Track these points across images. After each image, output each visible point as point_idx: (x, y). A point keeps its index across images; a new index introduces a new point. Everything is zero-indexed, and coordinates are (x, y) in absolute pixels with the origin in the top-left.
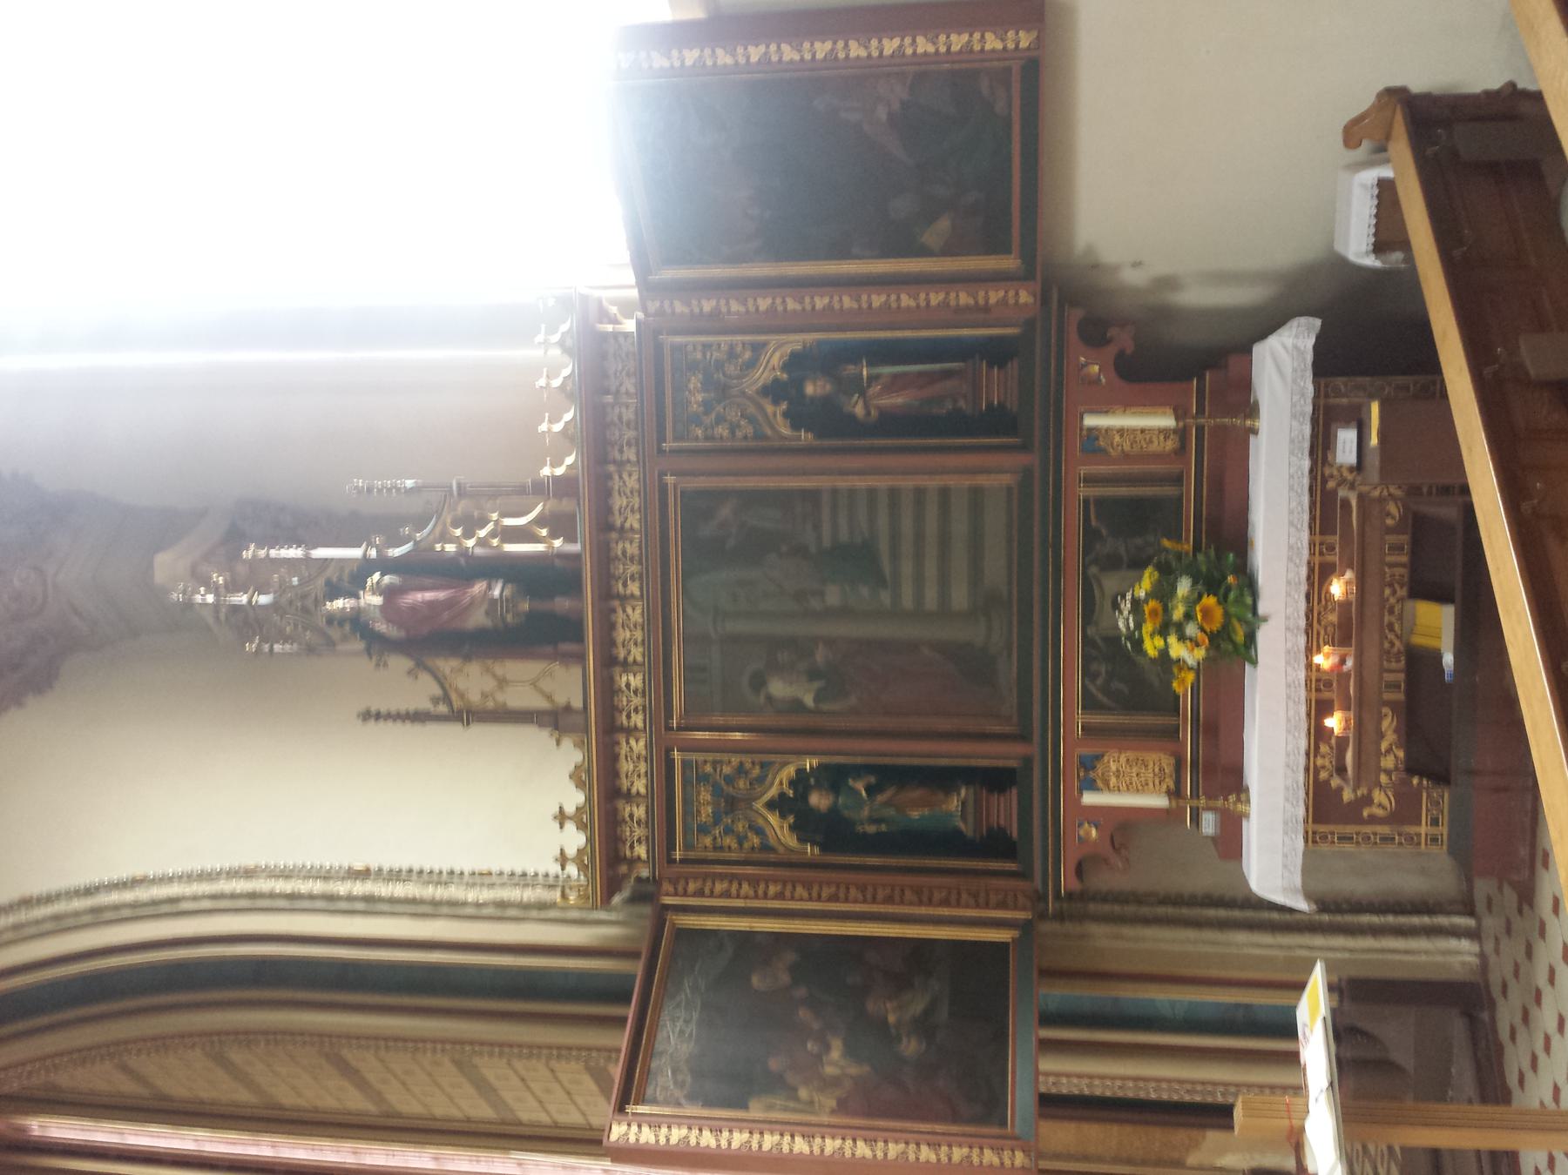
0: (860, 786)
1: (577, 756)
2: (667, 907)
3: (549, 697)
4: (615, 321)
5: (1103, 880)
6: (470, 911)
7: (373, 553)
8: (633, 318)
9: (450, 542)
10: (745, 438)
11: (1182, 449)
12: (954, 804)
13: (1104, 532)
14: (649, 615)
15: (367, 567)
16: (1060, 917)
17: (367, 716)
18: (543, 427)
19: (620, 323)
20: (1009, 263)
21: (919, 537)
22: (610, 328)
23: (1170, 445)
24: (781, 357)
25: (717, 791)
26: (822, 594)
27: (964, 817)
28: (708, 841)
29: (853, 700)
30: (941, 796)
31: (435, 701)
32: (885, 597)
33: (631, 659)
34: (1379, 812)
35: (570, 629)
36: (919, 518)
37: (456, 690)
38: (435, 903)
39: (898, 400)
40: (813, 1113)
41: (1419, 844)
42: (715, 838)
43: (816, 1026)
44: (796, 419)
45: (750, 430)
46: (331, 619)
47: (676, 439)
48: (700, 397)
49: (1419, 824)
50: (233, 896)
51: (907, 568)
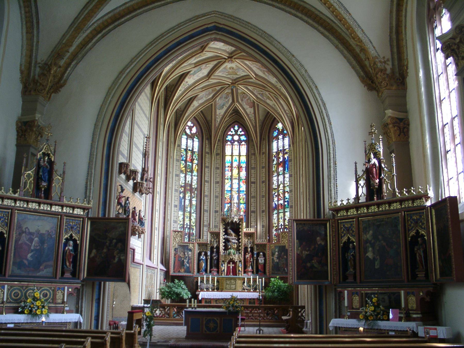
2: (330, 221)
6: (329, 185)
10: (408, 228)
12: (352, 270)
17: (356, 163)
18: (405, 189)
25: (350, 227)
28: (342, 226)
30: (352, 268)
38: (330, 179)
40: (297, 250)
43: (311, 249)
44: (413, 237)
47: (407, 214)
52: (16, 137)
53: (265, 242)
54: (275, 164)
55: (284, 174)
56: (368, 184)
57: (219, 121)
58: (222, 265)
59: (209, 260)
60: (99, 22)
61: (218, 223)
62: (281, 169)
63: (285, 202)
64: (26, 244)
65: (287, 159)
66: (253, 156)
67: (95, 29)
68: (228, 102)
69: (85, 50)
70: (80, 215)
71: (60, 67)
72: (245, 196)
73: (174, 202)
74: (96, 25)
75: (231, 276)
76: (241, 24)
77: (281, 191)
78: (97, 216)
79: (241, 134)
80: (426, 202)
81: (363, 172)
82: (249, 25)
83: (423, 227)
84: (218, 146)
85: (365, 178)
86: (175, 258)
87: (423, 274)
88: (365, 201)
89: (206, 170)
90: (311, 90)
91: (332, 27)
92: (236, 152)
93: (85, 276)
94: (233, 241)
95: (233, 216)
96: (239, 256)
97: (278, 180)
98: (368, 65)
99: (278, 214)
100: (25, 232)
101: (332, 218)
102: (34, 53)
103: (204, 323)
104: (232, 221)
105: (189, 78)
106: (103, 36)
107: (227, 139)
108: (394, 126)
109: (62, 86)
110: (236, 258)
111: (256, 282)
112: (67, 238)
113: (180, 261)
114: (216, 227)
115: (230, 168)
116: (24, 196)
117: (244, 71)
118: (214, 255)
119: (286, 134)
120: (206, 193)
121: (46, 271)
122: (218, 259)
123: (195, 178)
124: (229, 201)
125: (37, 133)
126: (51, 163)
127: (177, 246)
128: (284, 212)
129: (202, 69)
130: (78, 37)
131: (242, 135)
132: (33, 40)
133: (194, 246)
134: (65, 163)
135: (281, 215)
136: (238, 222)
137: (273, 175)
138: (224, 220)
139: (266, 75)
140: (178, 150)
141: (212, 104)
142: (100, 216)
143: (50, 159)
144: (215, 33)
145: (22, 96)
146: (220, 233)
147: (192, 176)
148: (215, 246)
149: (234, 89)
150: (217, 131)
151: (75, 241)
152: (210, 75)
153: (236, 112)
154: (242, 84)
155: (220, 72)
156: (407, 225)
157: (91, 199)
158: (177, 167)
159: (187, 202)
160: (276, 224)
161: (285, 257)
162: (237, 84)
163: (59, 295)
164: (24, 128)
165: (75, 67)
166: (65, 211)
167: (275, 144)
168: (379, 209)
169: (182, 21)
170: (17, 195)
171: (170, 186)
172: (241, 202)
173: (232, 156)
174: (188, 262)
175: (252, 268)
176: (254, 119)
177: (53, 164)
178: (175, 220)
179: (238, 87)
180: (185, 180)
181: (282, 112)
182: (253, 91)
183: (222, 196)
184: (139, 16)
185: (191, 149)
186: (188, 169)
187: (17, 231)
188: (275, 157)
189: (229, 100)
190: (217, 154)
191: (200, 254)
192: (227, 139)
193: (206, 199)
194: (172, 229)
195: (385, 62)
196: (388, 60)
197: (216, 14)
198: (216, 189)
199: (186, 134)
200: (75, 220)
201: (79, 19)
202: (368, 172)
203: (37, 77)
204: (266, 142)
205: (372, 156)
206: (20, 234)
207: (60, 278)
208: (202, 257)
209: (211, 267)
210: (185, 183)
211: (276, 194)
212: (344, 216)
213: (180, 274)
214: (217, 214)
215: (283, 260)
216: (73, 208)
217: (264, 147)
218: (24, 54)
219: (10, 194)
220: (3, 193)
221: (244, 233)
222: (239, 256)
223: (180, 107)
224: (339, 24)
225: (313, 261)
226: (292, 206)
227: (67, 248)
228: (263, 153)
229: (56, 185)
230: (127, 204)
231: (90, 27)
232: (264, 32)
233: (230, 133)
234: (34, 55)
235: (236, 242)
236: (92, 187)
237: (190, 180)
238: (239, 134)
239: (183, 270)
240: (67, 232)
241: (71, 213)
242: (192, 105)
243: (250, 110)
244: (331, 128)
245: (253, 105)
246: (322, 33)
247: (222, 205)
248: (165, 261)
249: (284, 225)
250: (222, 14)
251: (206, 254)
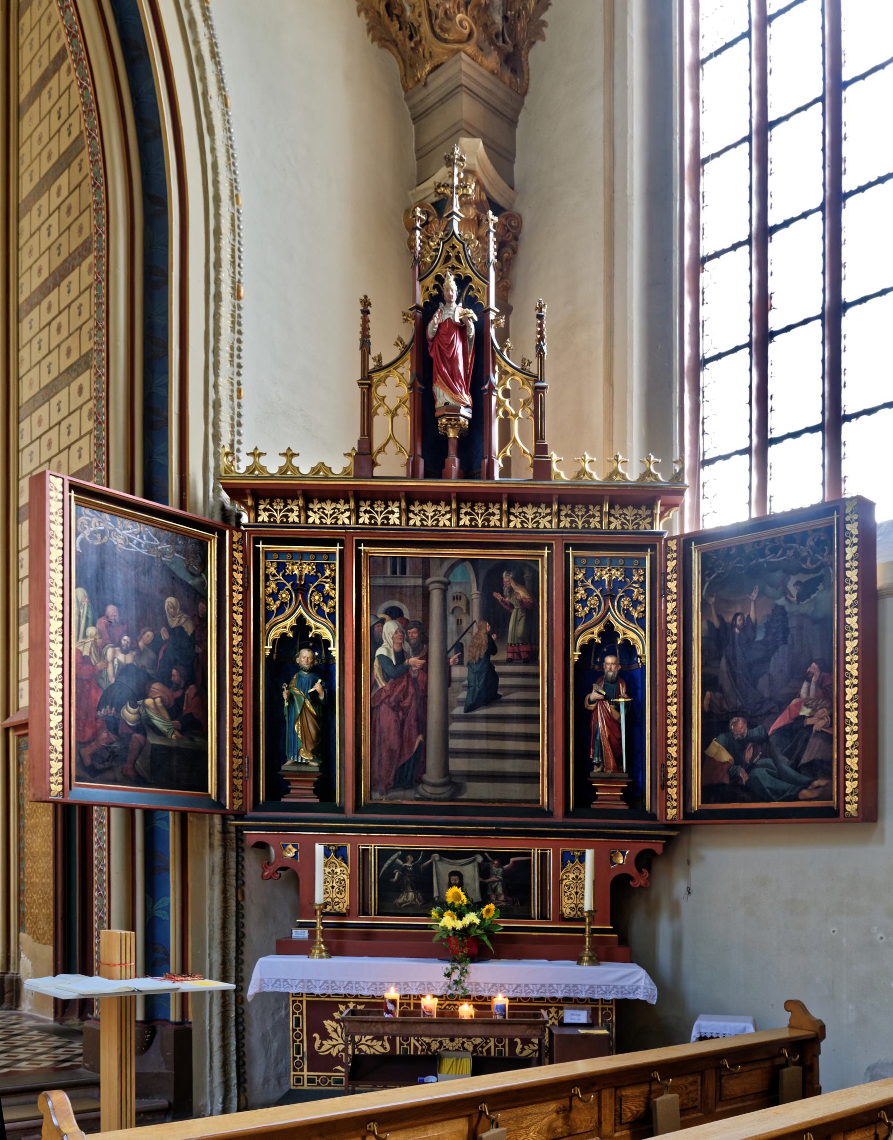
3: (382, 450)
4: (662, 516)
5: (252, 864)
7: (492, 316)
8: (664, 528)
9: (500, 378)
11: (563, 919)
12: (305, 756)
13: (506, 866)
14: (445, 531)
15: (483, 312)
16: (225, 831)
19: (661, 519)
20: (696, 801)
21: (502, 736)
22: (658, 510)
23: (567, 911)
24: (633, 639)
25: (310, 579)
26: (461, 663)
27: (296, 763)
28: (272, 570)
29: (381, 684)
32: (459, 710)
33: (411, 515)
34: (317, 1045)
35: (436, 470)
36: (516, 737)
37: (387, 377)
39: (601, 724)
41: (295, 1070)
42: (274, 575)
45: (581, 614)
46: (440, 279)
48: (606, 577)
49: (308, 1071)
51: (481, 727)
212: (285, 523)
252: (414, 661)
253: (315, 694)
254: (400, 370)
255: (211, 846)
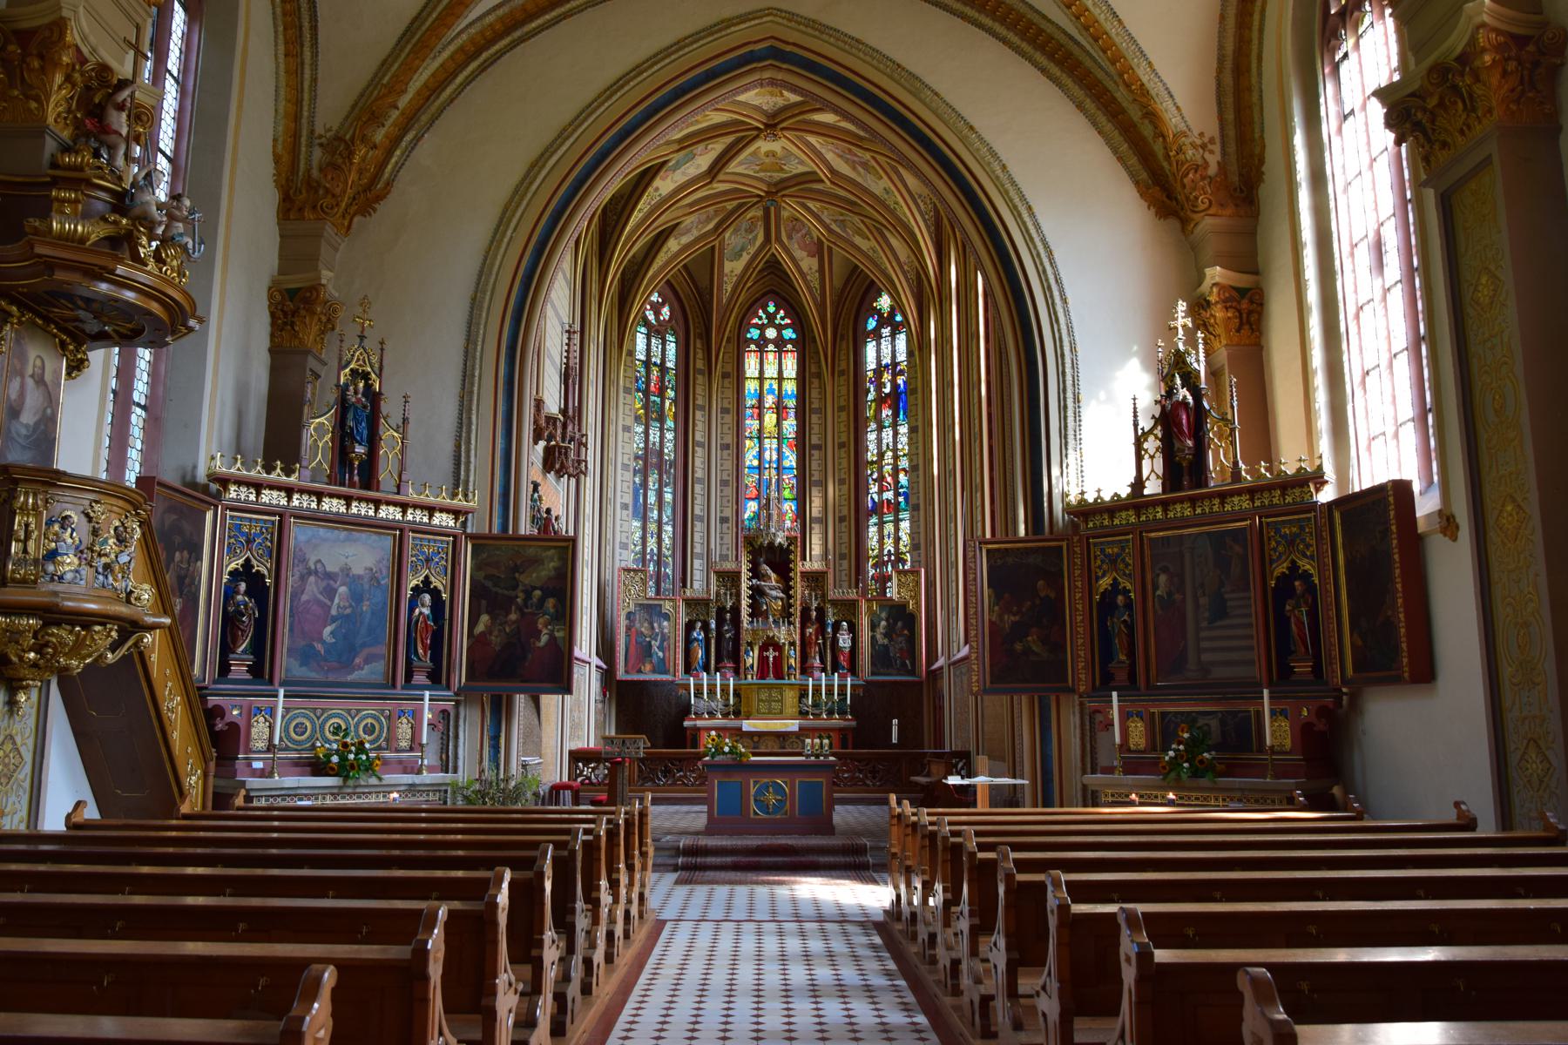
0: (1126, 617)
1: (1124, 495)
10: (1270, 555)
12: (1123, 658)
17: (1134, 399)
18: (1263, 463)
25: (1118, 555)
30: (1125, 652)
31: (1143, 429)
43: (1024, 610)
50: (1062, 347)
52: (269, 329)
53: (852, 595)
54: (871, 401)
55: (895, 425)
56: (1168, 450)
57: (729, 290)
58: (747, 653)
59: (713, 641)
60: (472, 31)
61: (728, 549)
62: (886, 412)
63: (897, 494)
64: (319, 602)
65: (902, 386)
66: (816, 382)
67: (461, 49)
68: (754, 243)
69: (437, 104)
70: (447, 527)
71: (375, 147)
72: (794, 481)
73: (622, 497)
74: (464, 37)
75: (771, 680)
76: (840, 44)
77: (888, 469)
78: (487, 532)
79: (783, 323)
80: (1317, 492)
81: (1152, 422)
82: (861, 46)
83: (1308, 553)
84: (727, 356)
85: (1160, 436)
86: (628, 635)
87: (1307, 666)
88: (1160, 490)
89: (699, 414)
90: (1018, 216)
91: (1069, 55)
92: (771, 371)
93: (463, 680)
94: (774, 593)
95: (773, 530)
96: (789, 630)
97: (879, 440)
98: (1160, 153)
99: (881, 525)
100: (316, 572)
101: (1070, 532)
102: (305, 108)
103: (753, 791)
104: (771, 544)
105: (663, 179)
106: (483, 68)
107: (749, 336)
108: (1227, 308)
109: (379, 198)
110: (782, 634)
111: (833, 694)
112: (417, 585)
113: (641, 643)
114: (724, 558)
115: (757, 411)
116: (312, 481)
117: (802, 162)
118: (726, 628)
119: (900, 323)
120: (699, 474)
121: (371, 671)
122: (736, 639)
123: (669, 436)
124: (755, 492)
125: (324, 319)
126: (374, 398)
127: (632, 608)
128: (897, 522)
129: (695, 155)
130: (421, 70)
131: (787, 326)
132: (302, 73)
133: (675, 607)
134: (406, 399)
135: (889, 528)
136: (785, 546)
137: (867, 427)
138: (750, 542)
139: (859, 174)
140: (629, 364)
141: (713, 248)
142: (495, 530)
143: (368, 387)
144: (771, 65)
145: (278, 224)
146: (740, 572)
147: (662, 430)
148: (729, 604)
149: (773, 208)
150: (723, 317)
151: (435, 594)
152: (715, 171)
153: (774, 266)
154: (798, 197)
155: (741, 164)
156: (1266, 548)
157: (471, 488)
158: (627, 407)
159: (652, 498)
160: (876, 552)
161: (906, 632)
162: (779, 194)
163: (404, 729)
164: (290, 305)
165: (413, 148)
166: (410, 517)
167: (870, 350)
168: (1195, 510)
169: (687, 33)
170: (293, 479)
171: (612, 455)
172: (787, 497)
173: (761, 378)
174: (660, 648)
175: (823, 660)
176: (818, 287)
177: (380, 400)
178: (624, 540)
179: (783, 205)
180: (647, 441)
181: (892, 267)
182: (820, 213)
183: (737, 482)
184: (575, 17)
185: (659, 362)
186: (653, 412)
187: (296, 569)
188: (871, 383)
189: (756, 235)
190: (725, 376)
191: (689, 627)
192: (749, 336)
193: (698, 488)
194: (617, 565)
195: (1204, 146)
196: (1212, 141)
197: (776, 15)
198: (722, 465)
199: (647, 323)
200: (435, 541)
201: (426, 20)
202: (1168, 418)
203: (315, 173)
204: (848, 348)
205: (1178, 381)
206: (303, 578)
207: (403, 688)
208: (695, 634)
209: (718, 661)
210: (646, 448)
211: (875, 476)
212: (1102, 527)
213: (641, 677)
214: (725, 525)
215: (900, 639)
216: (431, 510)
217: (843, 357)
218: (281, 111)
219: (277, 476)
220: (259, 472)
221: (802, 573)
222: (789, 630)
223: (634, 256)
224: (1088, 47)
225: (1030, 638)
226: (918, 505)
227: (417, 611)
228: (842, 373)
229: (388, 454)
230: (535, 501)
231: (449, 43)
232: (899, 65)
233: (756, 321)
234: (305, 114)
235: (781, 595)
236: (472, 459)
237: (658, 440)
238: (780, 324)
239: (648, 667)
240: (416, 572)
241: (425, 524)
242: (664, 249)
243: (809, 264)
244: (1067, 312)
245: (818, 250)
246: (1043, 71)
247: (737, 504)
248: (606, 648)
249: (898, 553)
250: (792, 16)
251: (706, 627)
252: (1177, 597)
253: (1125, 621)
254: (1155, 432)
255: (1074, 713)
